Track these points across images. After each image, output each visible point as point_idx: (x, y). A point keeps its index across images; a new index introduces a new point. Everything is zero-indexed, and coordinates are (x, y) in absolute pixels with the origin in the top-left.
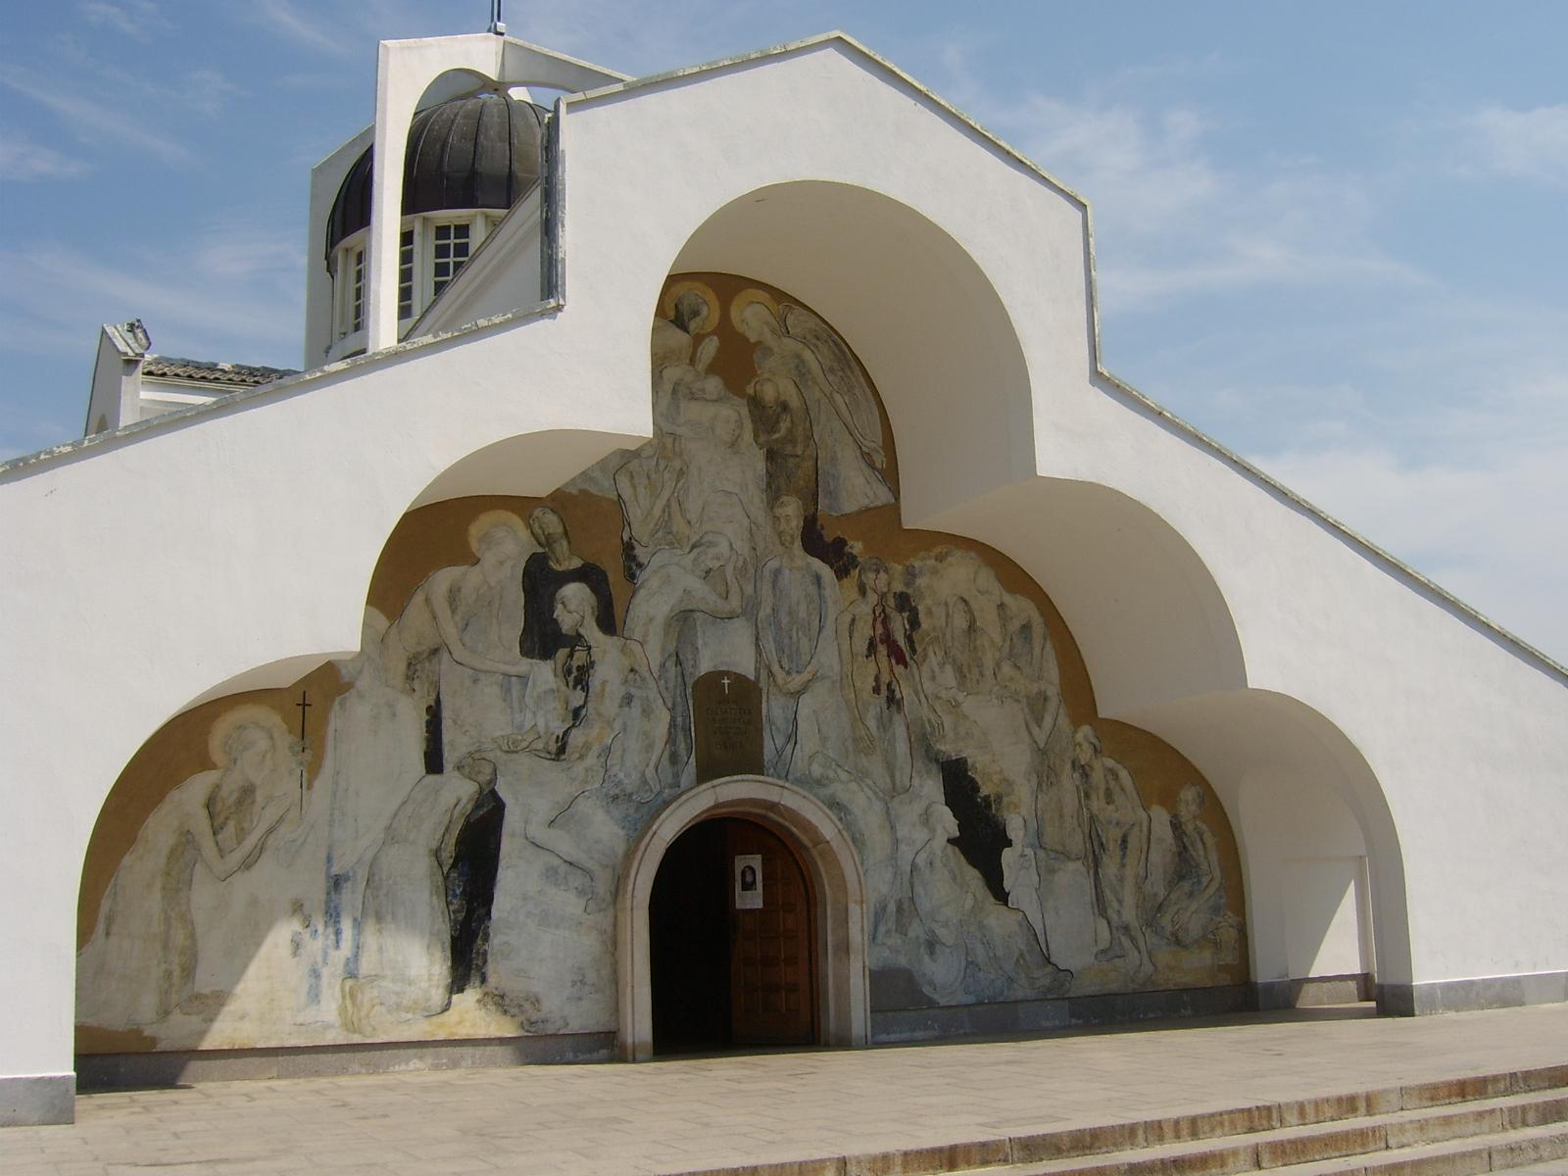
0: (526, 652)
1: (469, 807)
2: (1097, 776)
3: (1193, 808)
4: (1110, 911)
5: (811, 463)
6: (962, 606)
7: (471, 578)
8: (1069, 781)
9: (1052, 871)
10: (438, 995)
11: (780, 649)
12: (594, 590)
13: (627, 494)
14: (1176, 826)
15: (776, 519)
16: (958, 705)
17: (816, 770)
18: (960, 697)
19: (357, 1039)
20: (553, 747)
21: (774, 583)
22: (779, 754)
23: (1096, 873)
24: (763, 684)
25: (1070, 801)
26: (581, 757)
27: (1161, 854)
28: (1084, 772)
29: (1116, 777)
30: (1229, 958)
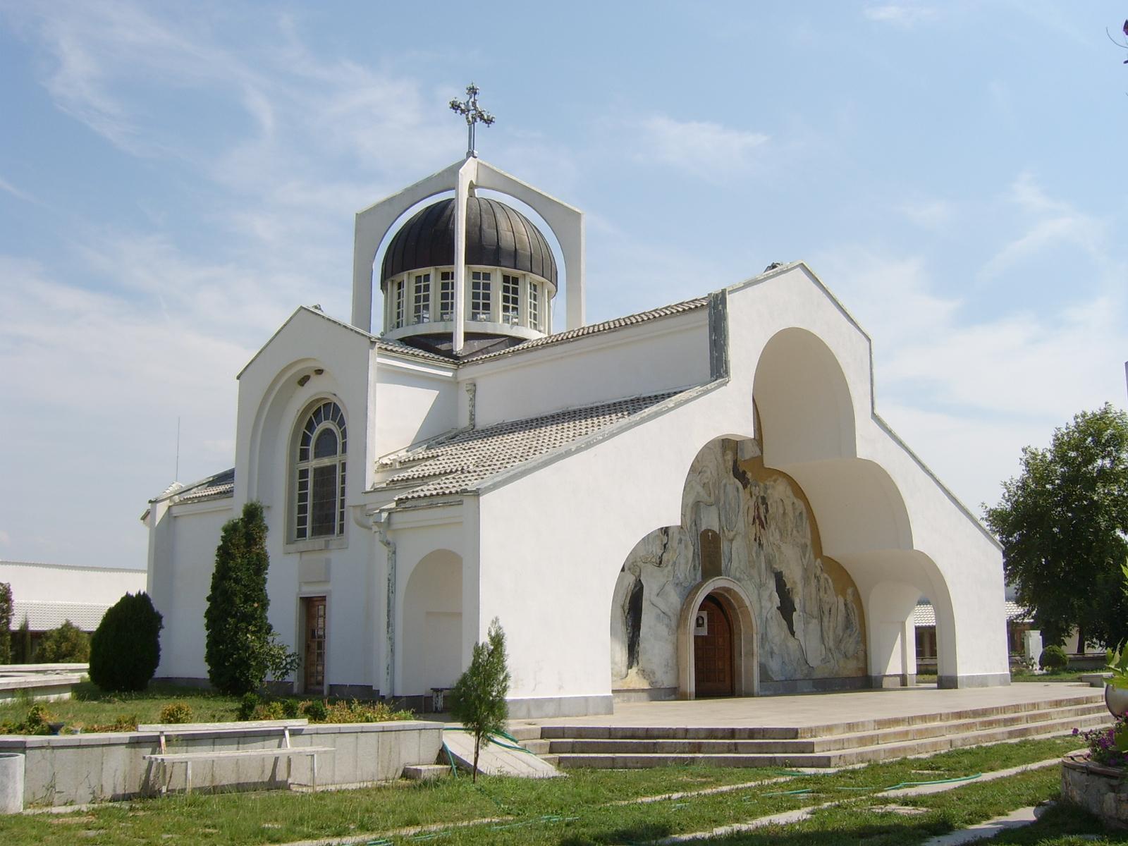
1: (633, 587)
2: (822, 580)
3: (851, 597)
8: (813, 582)
9: (808, 623)
10: (624, 669)
11: (726, 521)
15: (725, 461)
16: (779, 548)
17: (738, 575)
22: (726, 566)
24: (721, 536)
25: (814, 591)
26: (667, 566)
27: (841, 618)
30: (861, 665)
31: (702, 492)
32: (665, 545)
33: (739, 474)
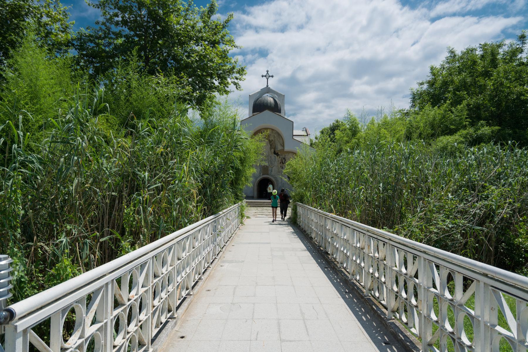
33: (275, 153)
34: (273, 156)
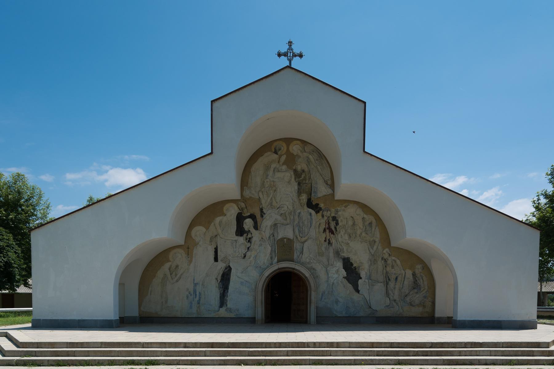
0: (237, 235)
2: (389, 262)
3: (420, 270)
4: (390, 296)
5: (310, 185)
6: (351, 219)
7: (224, 219)
8: (380, 263)
10: (217, 308)
11: (300, 232)
12: (253, 220)
13: (261, 196)
14: (414, 275)
16: (348, 244)
17: (308, 260)
18: (349, 242)
19: (200, 316)
20: (243, 256)
21: (299, 216)
23: (387, 286)
26: (249, 258)
28: (386, 261)
29: (395, 261)
31: (279, 218)
32: (248, 248)
34: (306, 212)
